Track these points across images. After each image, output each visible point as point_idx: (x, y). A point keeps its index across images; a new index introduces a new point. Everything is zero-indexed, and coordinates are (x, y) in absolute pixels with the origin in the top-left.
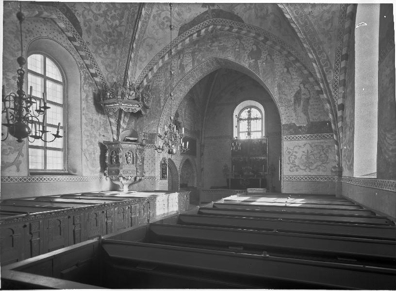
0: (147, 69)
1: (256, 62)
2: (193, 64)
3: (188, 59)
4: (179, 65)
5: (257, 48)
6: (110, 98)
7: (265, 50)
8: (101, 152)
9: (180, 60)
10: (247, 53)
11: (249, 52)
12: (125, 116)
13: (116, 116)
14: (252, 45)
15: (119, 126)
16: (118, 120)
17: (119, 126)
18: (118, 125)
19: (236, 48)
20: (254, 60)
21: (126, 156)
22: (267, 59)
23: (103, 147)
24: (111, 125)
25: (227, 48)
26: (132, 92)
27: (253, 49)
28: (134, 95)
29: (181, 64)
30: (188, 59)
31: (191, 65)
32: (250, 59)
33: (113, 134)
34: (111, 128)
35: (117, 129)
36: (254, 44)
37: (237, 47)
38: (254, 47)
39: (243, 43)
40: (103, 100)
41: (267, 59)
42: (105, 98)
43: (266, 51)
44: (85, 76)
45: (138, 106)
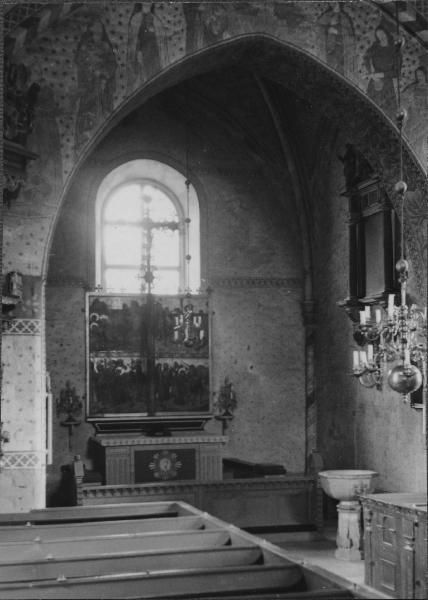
0: (15, 19)
1: (387, 80)
2: (190, 41)
3: (170, 18)
4: (136, 31)
5: (391, 39)
7: (411, 53)
9: (139, 16)
10: (362, 47)
11: (367, 47)
14: (375, 27)
19: (329, 26)
20: (381, 75)
22: (417, 82)
25: (303, 17)
27: (378, 41)
29: (143, 28)
30: (170, 18)
31: (183, 45)
32: (373, 69)
36: (380, 27)
37: (334, 22)
38: (381, 34)
39: (352, 15)
41: (417, 82)
43: (415, 57)
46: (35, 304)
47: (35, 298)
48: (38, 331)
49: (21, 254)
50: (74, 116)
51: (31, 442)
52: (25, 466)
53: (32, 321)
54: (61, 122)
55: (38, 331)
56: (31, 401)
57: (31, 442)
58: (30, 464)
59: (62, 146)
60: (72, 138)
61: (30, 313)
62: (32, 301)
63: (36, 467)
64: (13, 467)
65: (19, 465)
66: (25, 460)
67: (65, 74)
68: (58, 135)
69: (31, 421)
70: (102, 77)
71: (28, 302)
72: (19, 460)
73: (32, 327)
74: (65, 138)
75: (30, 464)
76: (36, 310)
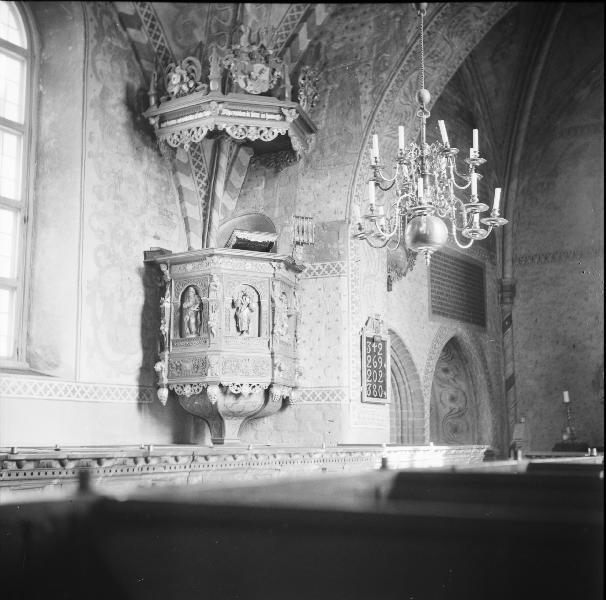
6: (181, 94)
8: (146, 296)
12: (231, 165)
13: (199, 167)
15: (209, 199)
16: (209, 181)
17: (209, 199)
18: (206, 198)
21: (233, 304)
23: (155, 273)
24: (182, 200)
26: (258, 67)
28: (265, 76)
33: (187, 229)
34: (184, 210)
35: (205, 215)
40: (158, 103)
42: (163, 93)
44: (100, 22)
45: (278, 117)
46: (341, 247)
47: (341, 241)
48: (344, 272)
49: (328, 202)
50: (371, 63)
51: (338, 378)
52: (333, 401)
53: (338, 262)
54: (360, 71)
55: (344, 272)
56: (338, 338)
57: (338, 378)
58: (338, 400)
59: (360, 94)
60: (369, 83)
61: (336, 255)
62: (339, 244)
63: (343, 401)
64: (323, 401)
65: (328, 400)
66: (333, 395)
67: (363, 25)
68: (358, 84)
69: (338, 358)
70: (396, 16)
71: (335, 246)
72: (328, 395)
73: (338, 269)
74: (364, 85)
75: (338, 400)
76: (341, 253)
